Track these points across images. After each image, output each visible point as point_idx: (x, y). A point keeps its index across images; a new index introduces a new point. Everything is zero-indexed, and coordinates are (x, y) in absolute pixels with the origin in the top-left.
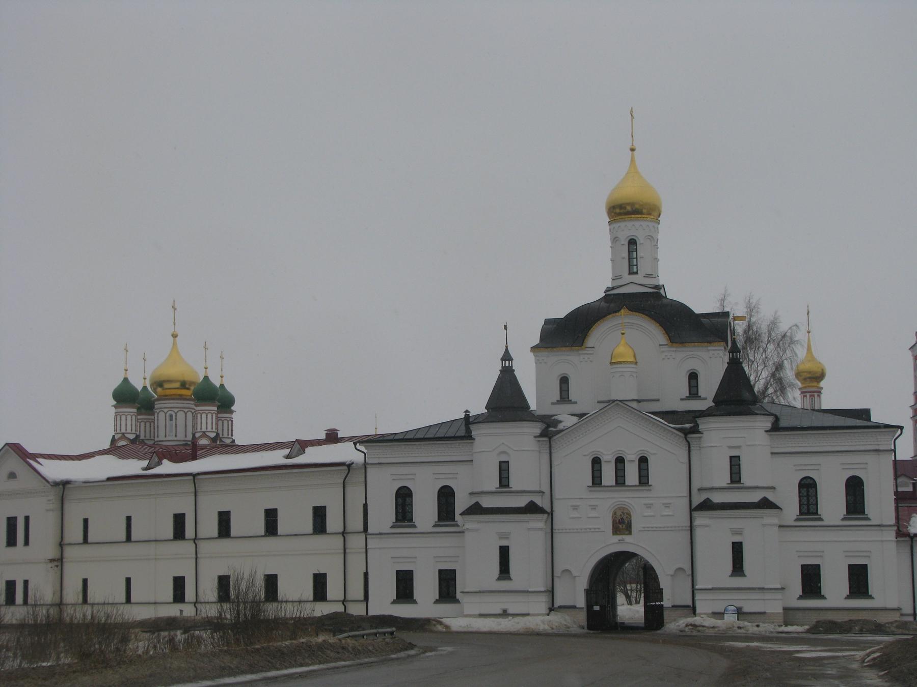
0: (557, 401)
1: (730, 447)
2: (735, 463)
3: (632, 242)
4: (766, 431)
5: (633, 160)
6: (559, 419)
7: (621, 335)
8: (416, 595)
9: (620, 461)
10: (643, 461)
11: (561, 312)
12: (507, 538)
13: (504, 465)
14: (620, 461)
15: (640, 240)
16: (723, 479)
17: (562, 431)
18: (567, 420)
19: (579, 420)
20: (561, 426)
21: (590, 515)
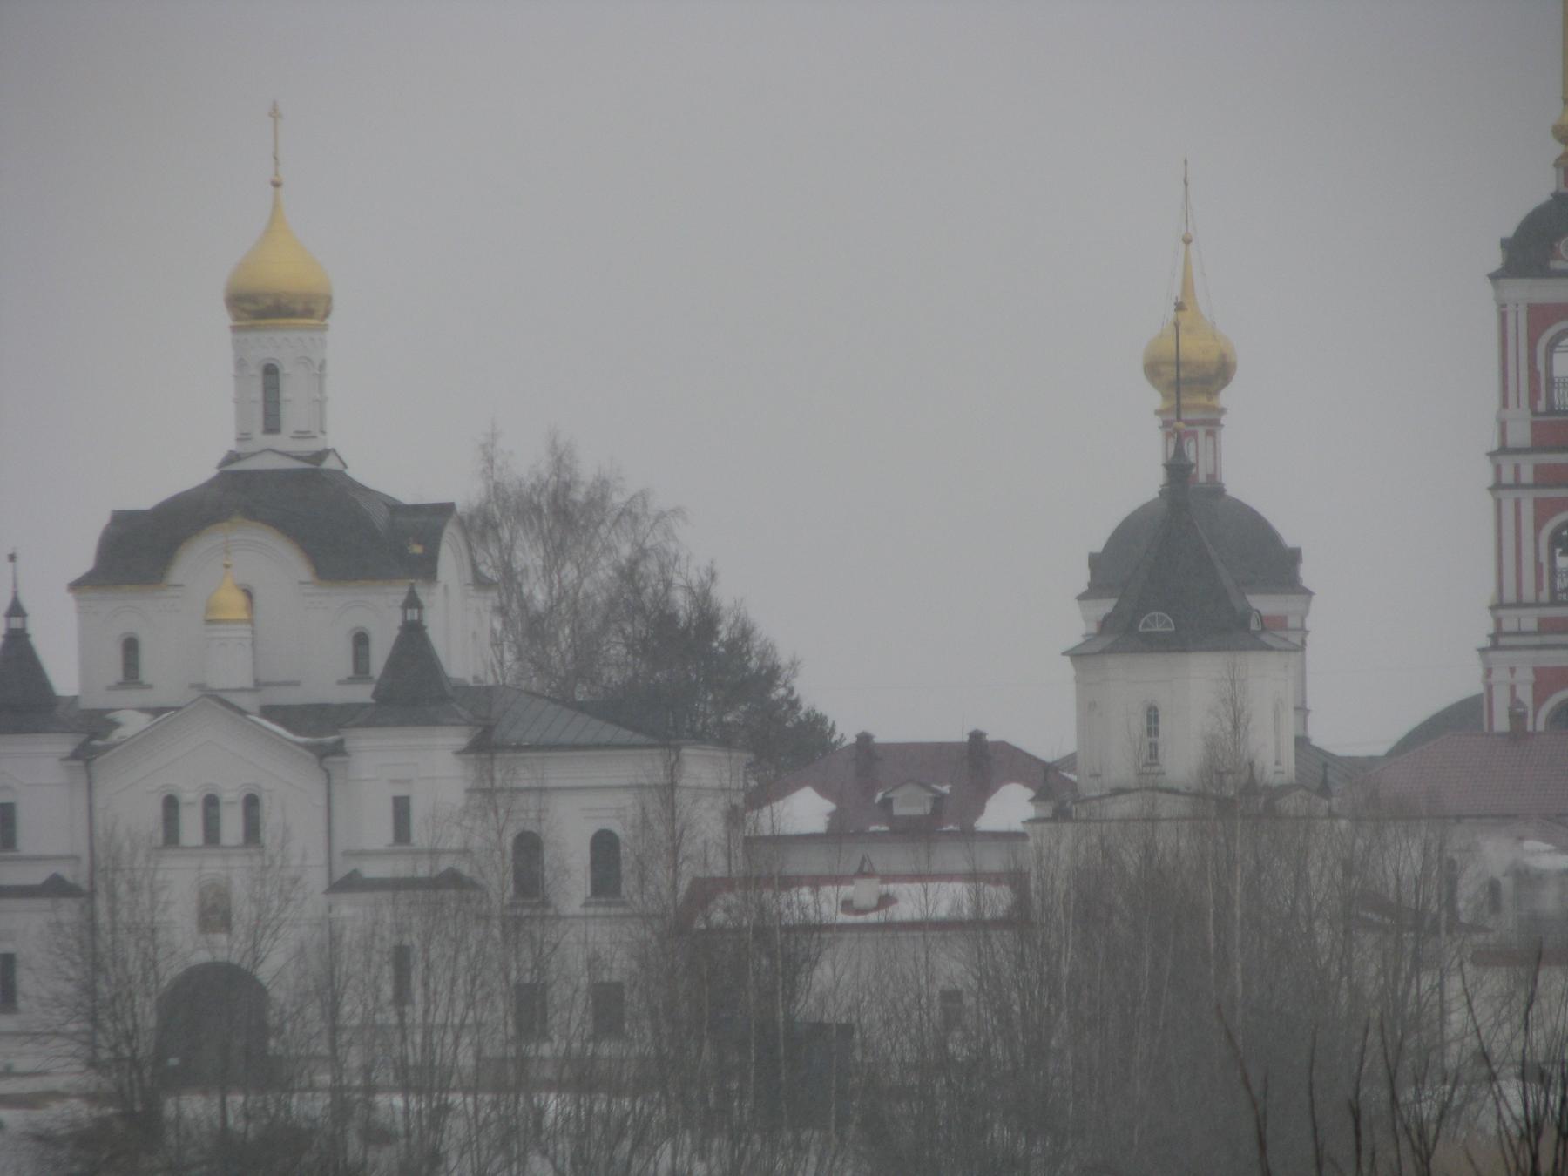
2: (401, 807)
5: (276, 206)
11: (146, 498)
16: (379, 832)
17: (115, 745)
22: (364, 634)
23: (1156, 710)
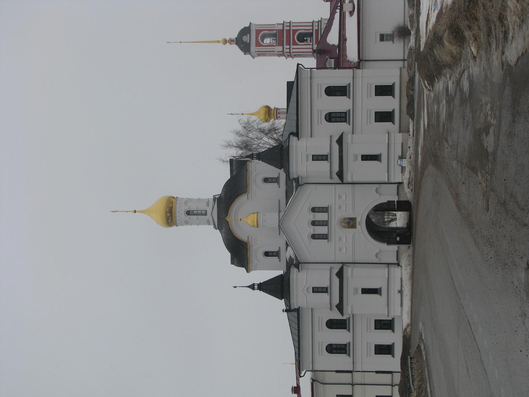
0: (278, 184)
1: (307, 160)
2: (316, 158)
3: (188, 213)
4: (298, 140)
5: (141, 212)
6: (289, 257)
7: (241, 221)
8: (390, 84)
9: (314, 223)
10: (314, 210)
11: (227, 255)
12: (357, 156)
13: (315, 158)
14: (314, 223)
15: (187, 208)
16: (324, 165)
17: (295, 256)
18: (290, 253)
19: (289, 246)
20: (293, 257)
21: (344, 199)
22: (264, 181)
23: (330, 114)
